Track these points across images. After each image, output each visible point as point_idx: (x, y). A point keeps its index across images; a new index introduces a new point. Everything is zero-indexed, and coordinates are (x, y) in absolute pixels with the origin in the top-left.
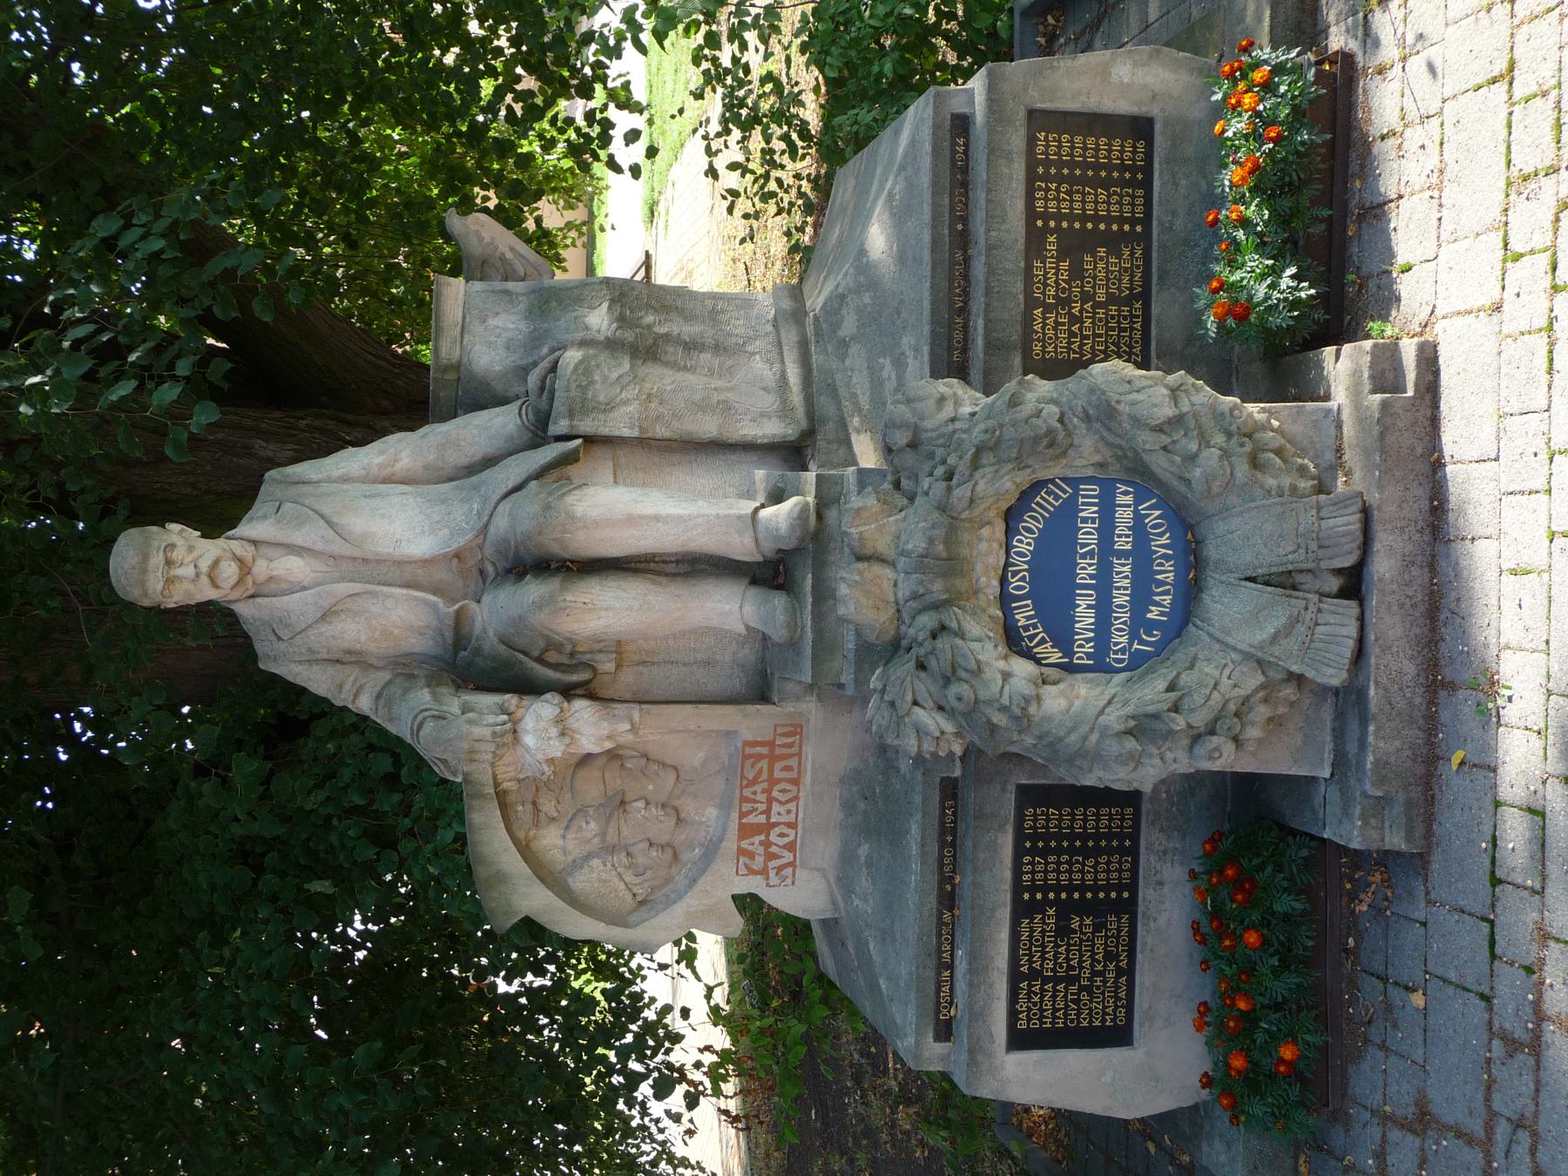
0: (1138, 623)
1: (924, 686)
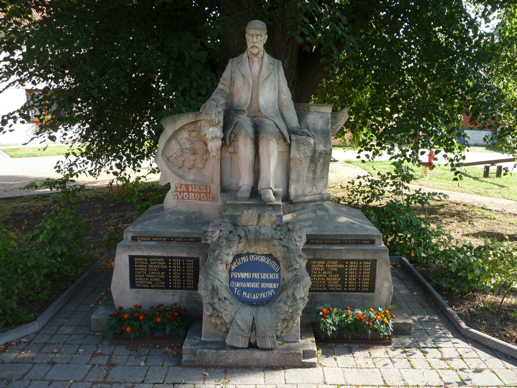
0: (242, 289)
1: (225, 233)
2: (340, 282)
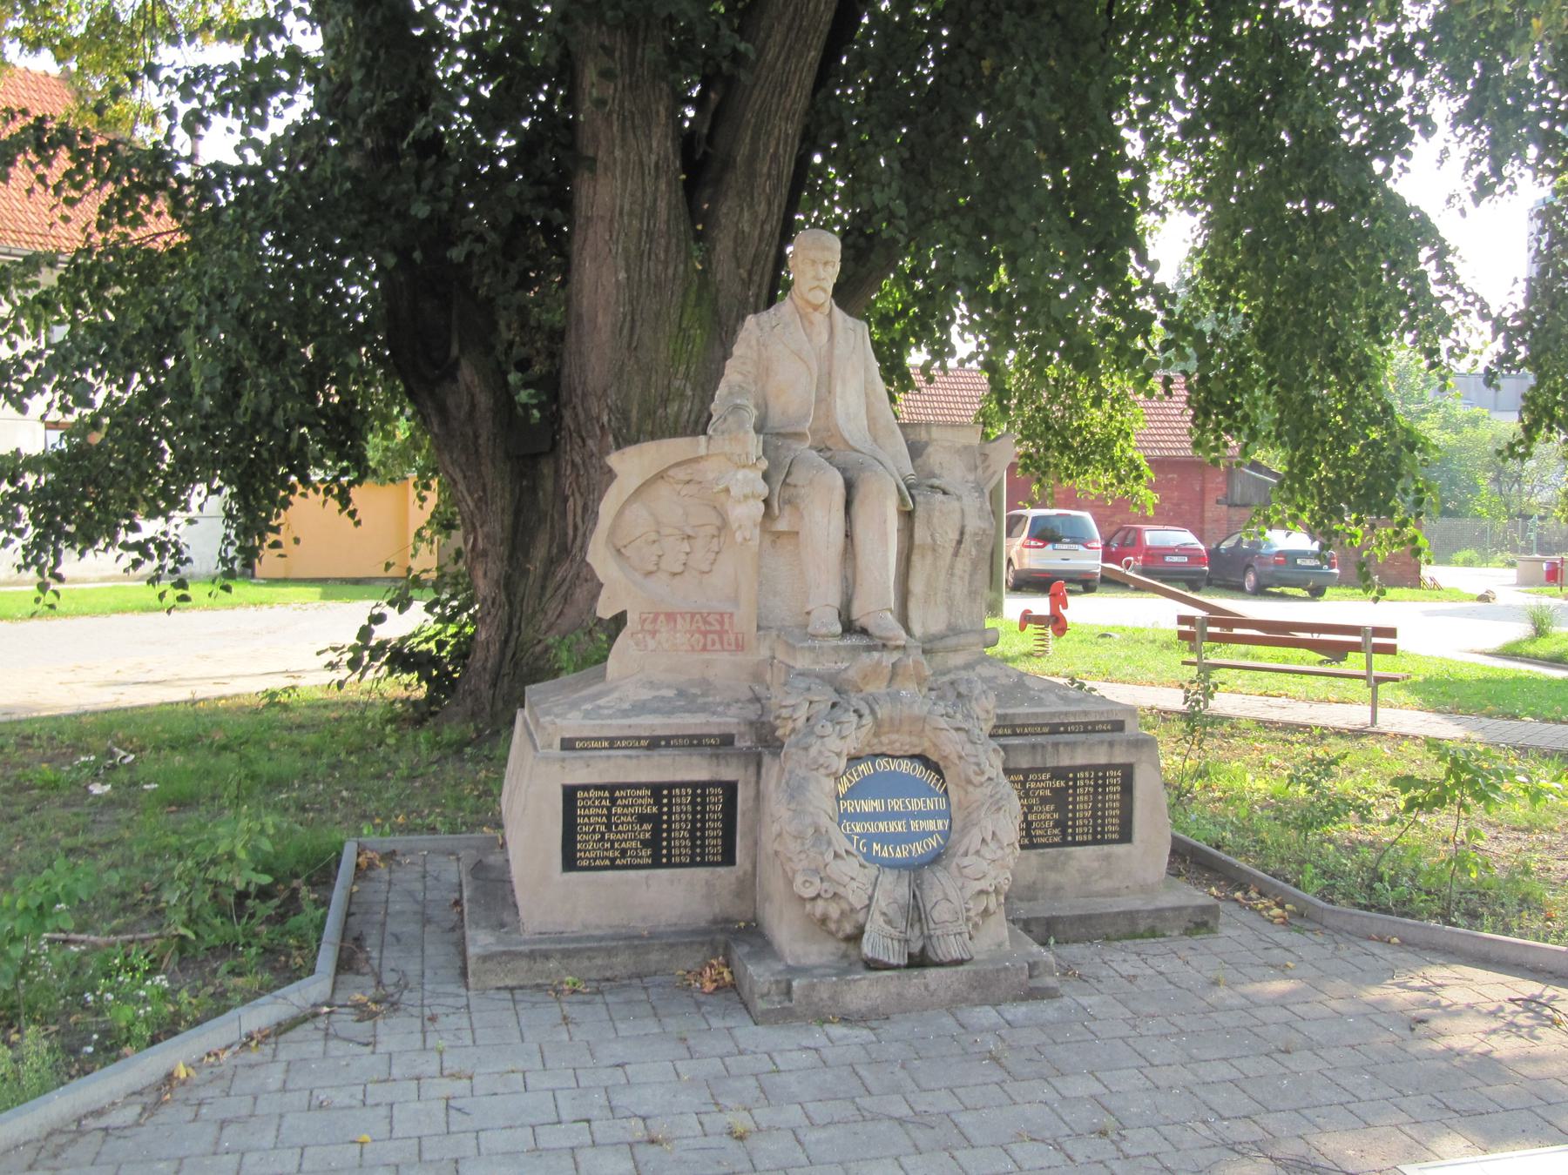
0: (870, 838)
1: (824, 707)
2: (1057, 824)
